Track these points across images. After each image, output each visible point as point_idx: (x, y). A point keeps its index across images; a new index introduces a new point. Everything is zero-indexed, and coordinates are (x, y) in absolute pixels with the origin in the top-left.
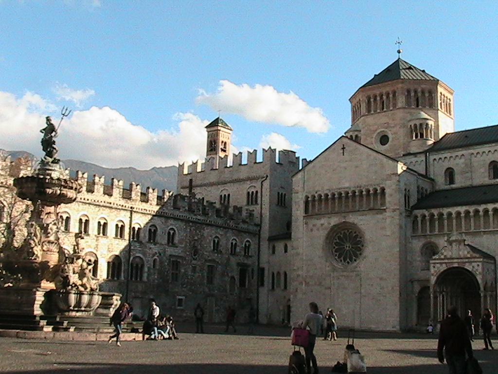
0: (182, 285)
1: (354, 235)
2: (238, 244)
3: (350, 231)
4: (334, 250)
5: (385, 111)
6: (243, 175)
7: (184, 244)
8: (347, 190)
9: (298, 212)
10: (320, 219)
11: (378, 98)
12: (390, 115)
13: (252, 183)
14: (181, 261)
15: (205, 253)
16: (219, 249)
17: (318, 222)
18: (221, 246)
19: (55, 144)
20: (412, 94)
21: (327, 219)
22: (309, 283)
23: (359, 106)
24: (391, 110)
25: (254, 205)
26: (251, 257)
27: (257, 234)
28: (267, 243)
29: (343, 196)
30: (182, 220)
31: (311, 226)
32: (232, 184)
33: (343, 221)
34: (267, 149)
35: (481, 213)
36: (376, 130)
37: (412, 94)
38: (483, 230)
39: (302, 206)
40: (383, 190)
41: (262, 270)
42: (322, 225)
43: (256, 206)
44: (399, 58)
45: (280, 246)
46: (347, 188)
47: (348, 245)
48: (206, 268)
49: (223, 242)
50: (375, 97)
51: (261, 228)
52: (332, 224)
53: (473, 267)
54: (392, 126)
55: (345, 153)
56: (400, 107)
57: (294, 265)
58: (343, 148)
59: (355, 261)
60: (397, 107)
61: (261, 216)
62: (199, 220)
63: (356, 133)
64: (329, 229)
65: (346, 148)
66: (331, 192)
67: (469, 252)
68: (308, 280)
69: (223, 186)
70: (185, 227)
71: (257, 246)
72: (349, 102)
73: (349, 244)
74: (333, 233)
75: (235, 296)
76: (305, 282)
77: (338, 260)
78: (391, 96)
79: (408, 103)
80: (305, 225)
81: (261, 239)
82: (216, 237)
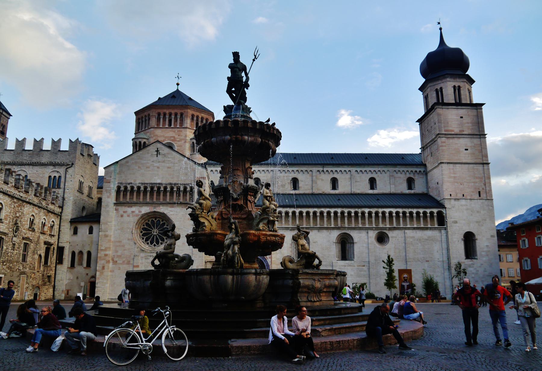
0: (3, 262)
1: (161, 223)
2: (47, 223)
3: (157, 219)
5: (172, 128)
6: (44, 160)
7: (8, 220)
9: (109, 199)
10: (131, 207)
11: (167, 116)
13: (55, 168)
14: (4, 238)
15: (23, 231)
16: (33, 226)
17: (129, 210)
18: (35, 225)
19: (247, 89)
20: (195, 119)
21: (138, 207)
22: (117, 261)
23: (147, 118)
24: (178, 128)
25: (56, 188)
26: (54, 236)
27: (59, 216)
28: (70, 223)
29: (155, 190)
30: (9, 196)
31: (121, 212)
32: (31, 166)
34: (73, 141)
37: (195, 119)
39: (114, 194)
41: (61, 250)
42: (133, 212)
43: (58, 190)
44: (178, 90)
45: (83, 229)
46: (159, 184)
47: (155, 231)
48: (22, 245)
49: (36, 221)
50: (165, 114)
51: (62, 210)
52: (143, 212)
54: (178, 140)
56: (185, 126)
57: (102, 246)
58: (157, 151)
59: (161, 244)
60: (183, 126)
61: (64, 199)
62: (21, 197)
63: (145, 140)
64: (140, 216)
65: (160, 152)
66: (143, 185)
68: (115, 259)
69: (19, 166)
70: (10, 203)
71: (58, 226)
74: (142, 220)
75: (40, 273)
76: (113, 260)
77: (145, 242)
78: (179, 117)
79: (191, 125)
80: (115, 211)
81: (62, 220)
82: (33, 215)
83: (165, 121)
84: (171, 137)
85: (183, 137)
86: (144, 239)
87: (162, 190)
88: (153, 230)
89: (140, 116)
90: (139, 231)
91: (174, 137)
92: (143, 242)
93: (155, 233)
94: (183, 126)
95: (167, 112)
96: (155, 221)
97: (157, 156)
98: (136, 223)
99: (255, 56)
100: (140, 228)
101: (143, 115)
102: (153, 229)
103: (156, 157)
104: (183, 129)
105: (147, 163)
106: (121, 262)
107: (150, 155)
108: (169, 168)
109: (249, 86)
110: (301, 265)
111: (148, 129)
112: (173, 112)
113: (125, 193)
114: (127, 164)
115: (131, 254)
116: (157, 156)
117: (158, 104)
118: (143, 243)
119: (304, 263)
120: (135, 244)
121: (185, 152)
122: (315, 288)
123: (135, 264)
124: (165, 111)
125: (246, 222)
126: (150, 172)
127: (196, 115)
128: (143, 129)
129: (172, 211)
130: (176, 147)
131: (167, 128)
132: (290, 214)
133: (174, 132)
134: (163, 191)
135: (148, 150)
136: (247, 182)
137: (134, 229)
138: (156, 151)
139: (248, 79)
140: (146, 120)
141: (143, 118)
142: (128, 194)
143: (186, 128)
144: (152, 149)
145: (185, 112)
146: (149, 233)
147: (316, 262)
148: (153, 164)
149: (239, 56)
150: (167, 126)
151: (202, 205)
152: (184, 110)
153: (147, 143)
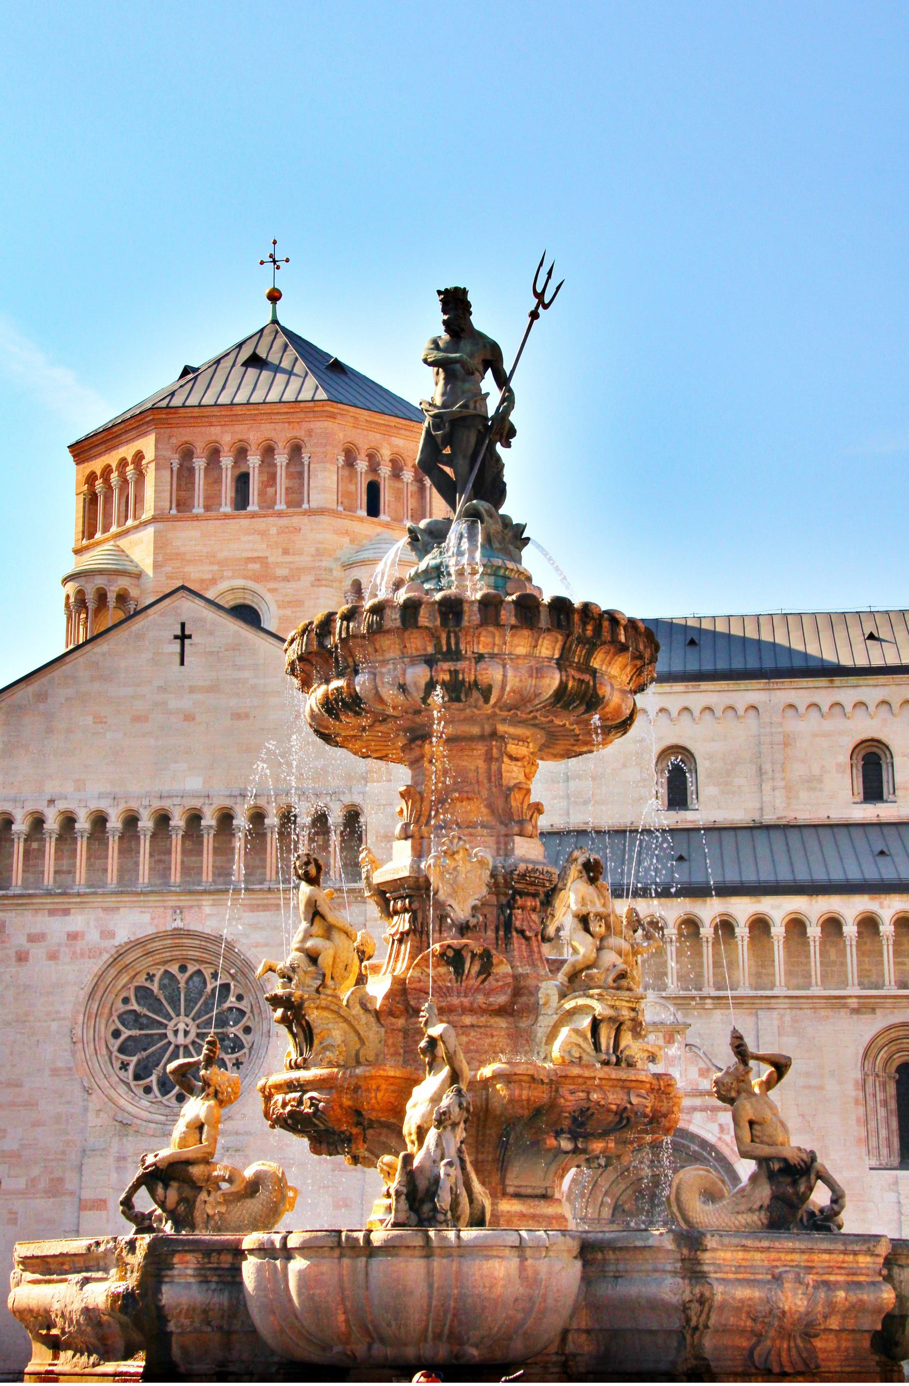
3: (192, 968)
4: (116, 1043)
8: (196, 803)
10: (66, 912)
11: (227, 461)
19: (507, 445)
20: (362, 465)
24: (280, 514)
29: (177, 828)
33: (175, 925)
35: (707, 931)
36: (214, 581)
37: (362, 465)
38: (714, 993)
42: (73, 936)
44: (275, 321)
46: (196, 796)
47: (182, 1026)
52: (123, 936)
53: (721, 1126)
54: (281, 572)
56: (314, 505)
58: (183, 637)
64: (106, 956)
66: (122, 807)
67: (708, 1070)
73: (188, 1020)
78: (281, 459)
83: (218, 481)
85: (304, 560)
86: (131, 1068)
87: (211, 827)
88: (171, 1024)
90: (104, 1031)
91: (262, 560)
92: (127, 1085)
93: (181, 1034)
94: (305, 506)
96: (179, 976)
97: (182, 663)
98: (88, 990)
99: (539, 296)
100: (111, 1014)
101: (112, 459)
102: (171, 1019)
104: (306, 519)
106: (21, 1183)
108: (238, 716)
109: (512, 432)
110: (750, 1210)
111: (136, 528)
112: (255, 436)
113: (35, 845)
114: (42, 707)
115: (68, 1143)
116: (182, 663)
117: (177, 401)
118: (122, 1089)
119: (767, 1202)
120: (88, 1091)
122: (784, 1313)
123: (87, 1194)
124: (215, 431)
125: (504, 1025)
126: (152, 742)
129: (263, 928)
130: (273, 607)
131: (226, 516)
132: (850, 930)
133: (263, 534)
134: (212, 832)
135: (139, 637)
136: (508, 853)
137: (81, 1017)
138: (176, 637)
139: (508, 400)
140: (125, 481)
141: (111, 471)
142: (50, 847)
143: (321, 511)
145: (310, 433)
146: (150, 1040)
147: (820, 1197)
148: (165, 703)
149: (468, 305)
150: (227, 508)
151: (320, 960)
152: (305, 425)
153: (134, 592)
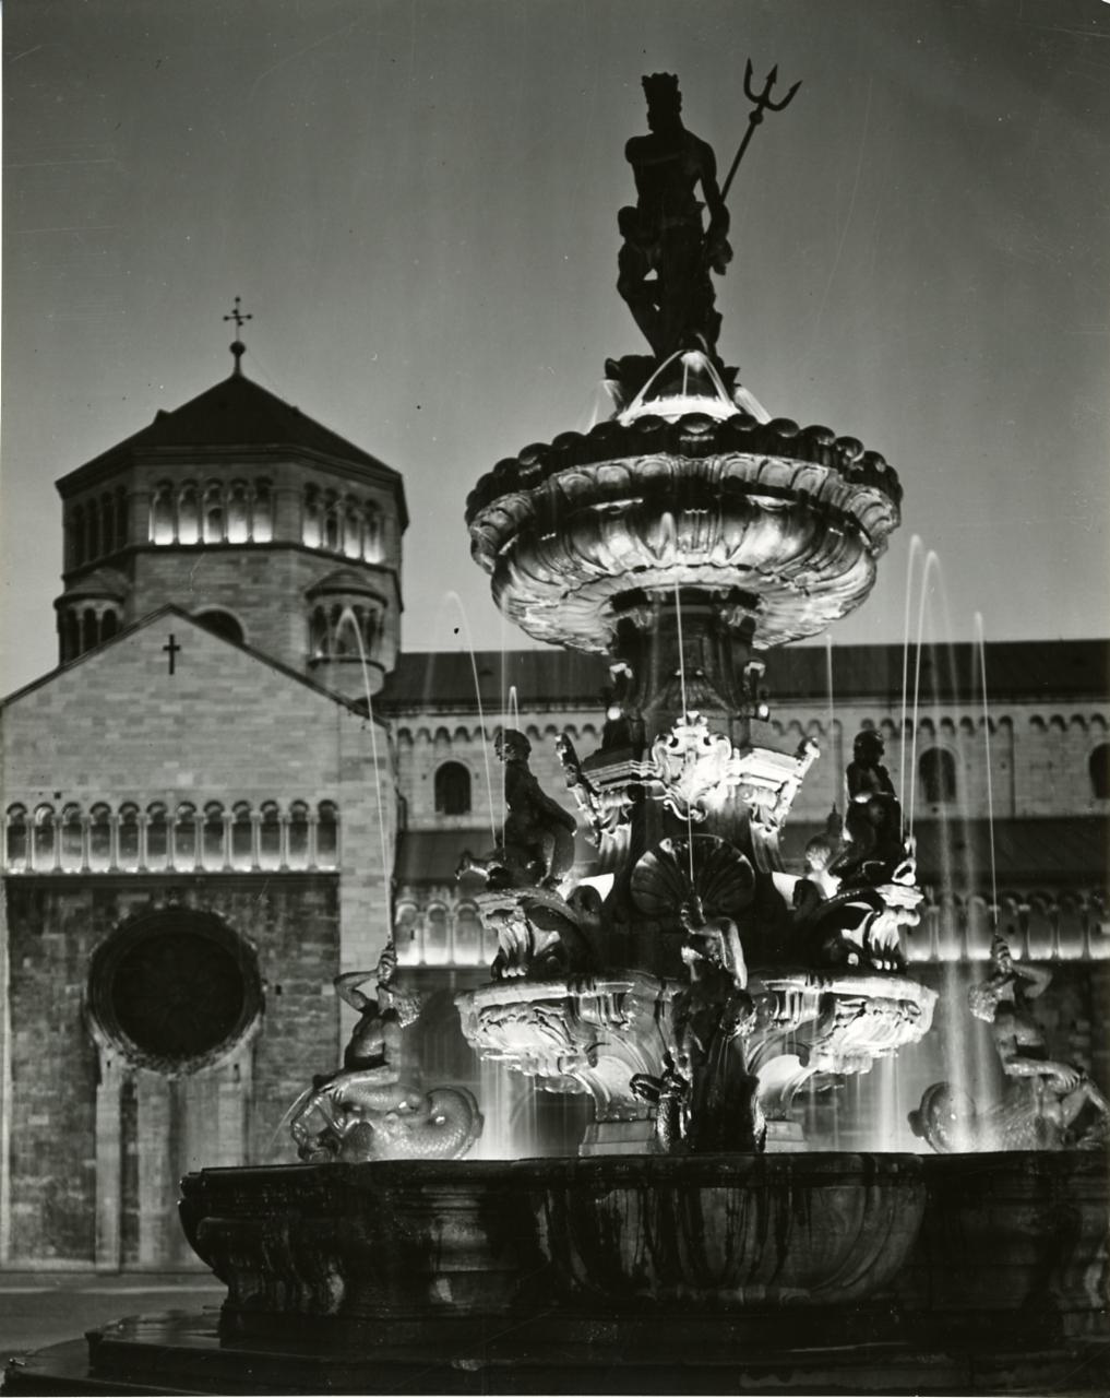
12: (244, 561)
40: (327, 807)
54: (252, 598)
55: (177, 669)
58: (172, 649)
63: (108, 605)
65: (185, 651)
72: (56, 495)
84: (222, 587)
89: (82, 499)
91: (234, 587)
95: (201, 475)
103: (166, 675)
105: (134, 702)
107: (141, 664)
114: (46, 710)
116: (172, 671)
121: (286, 651)
126: (147, 742)
127: (323, 486)
128: (100, 557)
133: (236, 563)
144: (150, 640)
153: (120, 615)
